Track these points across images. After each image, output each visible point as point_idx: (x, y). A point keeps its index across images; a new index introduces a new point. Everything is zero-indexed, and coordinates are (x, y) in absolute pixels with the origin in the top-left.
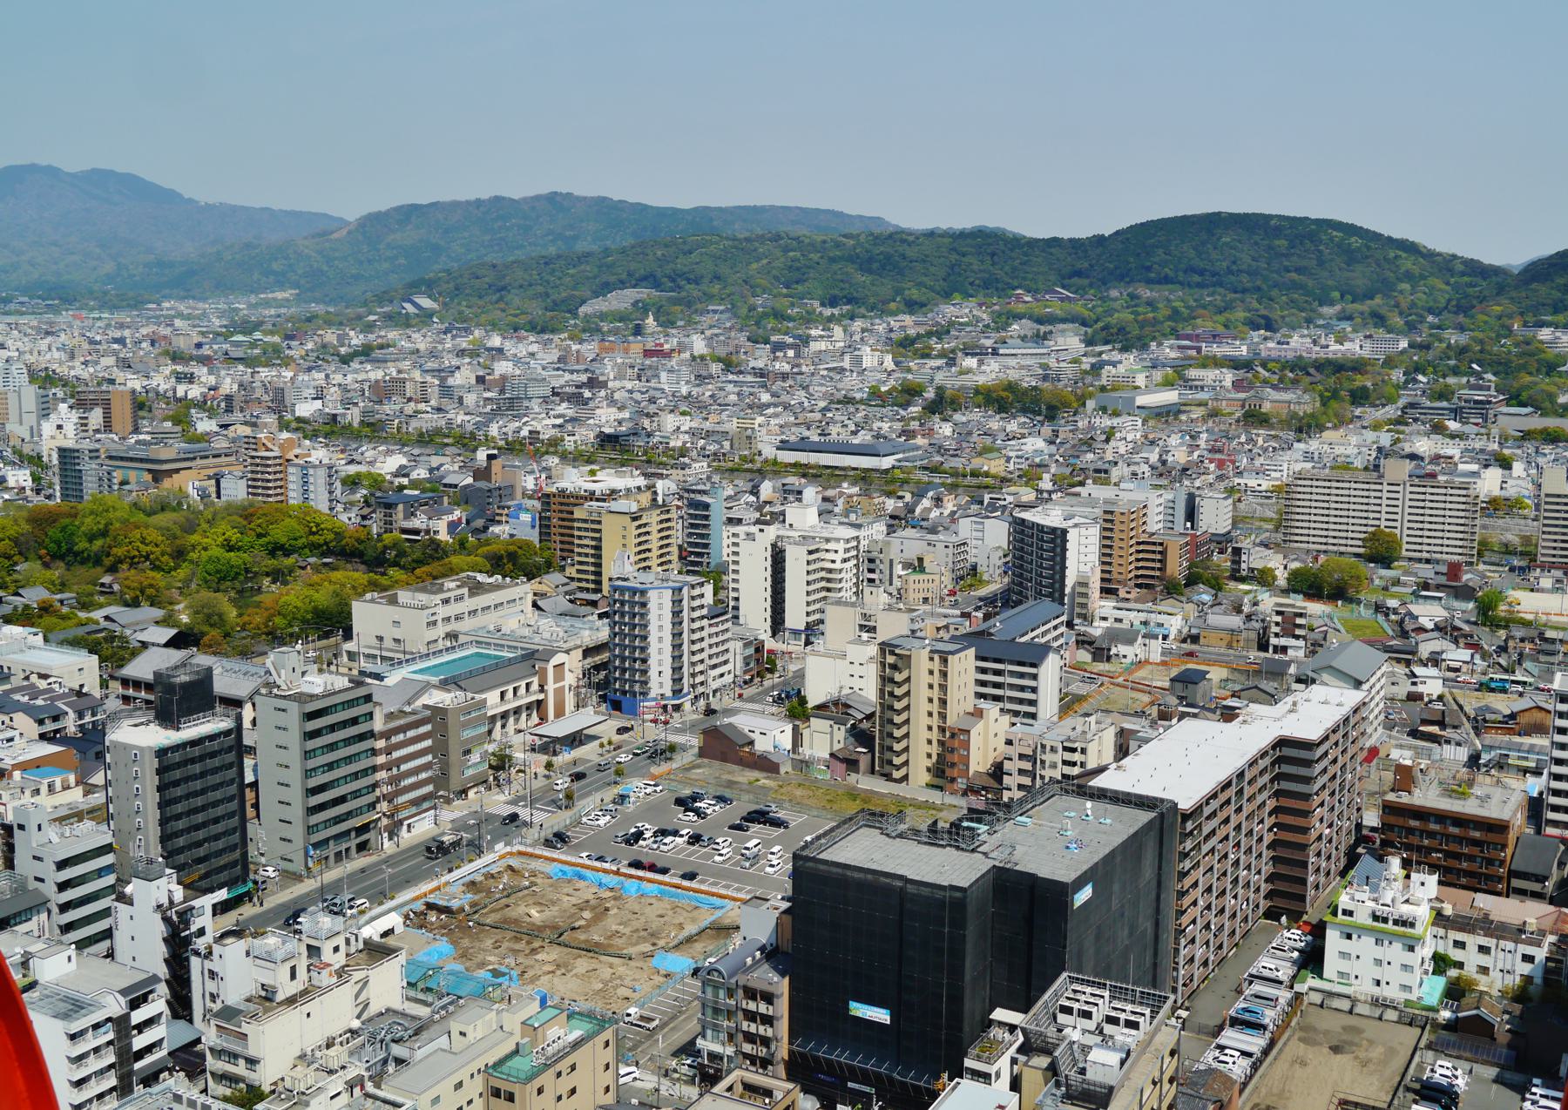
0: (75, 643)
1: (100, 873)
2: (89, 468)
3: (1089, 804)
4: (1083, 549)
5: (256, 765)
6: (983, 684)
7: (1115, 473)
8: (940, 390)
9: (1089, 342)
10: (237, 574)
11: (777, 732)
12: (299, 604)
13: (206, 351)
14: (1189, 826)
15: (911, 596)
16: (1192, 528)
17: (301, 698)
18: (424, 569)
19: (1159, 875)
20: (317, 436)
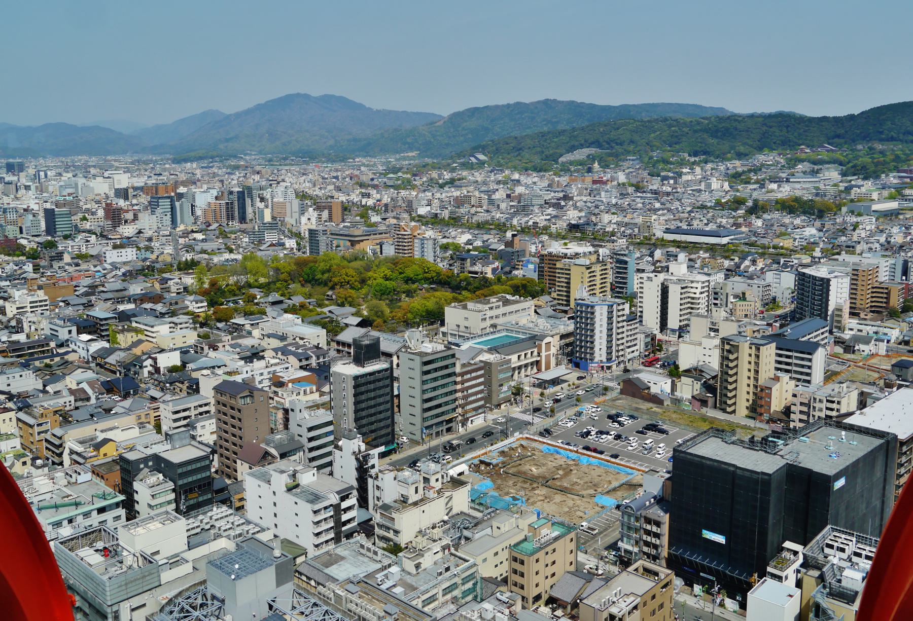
0: (315, 323)
1: (327, 434)
2: (322, 239)
3: (843, 433)
4: (839, 290)
5: (399, 386)
6: (780, 362)
7: (859, 248)
8: (756, 201)
9: (844, 174)
10: (390, 292)
11: (663, 383)
12: (419, 308)
13: (376, 182)
14: (905, 449)
15: (738, 313)
16: (906, 280)
17: (421, 354)
18: (480, 292)
19: (885, 475)
20: (428, 224)
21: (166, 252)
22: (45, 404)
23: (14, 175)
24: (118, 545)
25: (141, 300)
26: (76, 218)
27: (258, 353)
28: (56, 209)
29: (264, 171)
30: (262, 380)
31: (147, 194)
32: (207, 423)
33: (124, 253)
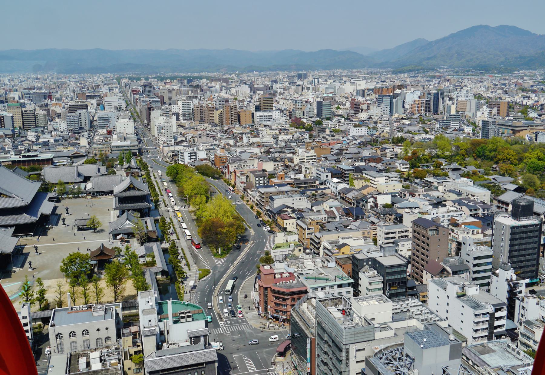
1: (488, 264)
21: (385, 131)
22: (312, 217)
23: (301, 81)
24: (351, 309)
25: (369, 160)
26: (334, 107)
27: (441, 202)
28: (323, 102)
29: (452, 79)
30: (443, 220)
31: (376, 94)
32: (405, 243)
33: (360, 131)
